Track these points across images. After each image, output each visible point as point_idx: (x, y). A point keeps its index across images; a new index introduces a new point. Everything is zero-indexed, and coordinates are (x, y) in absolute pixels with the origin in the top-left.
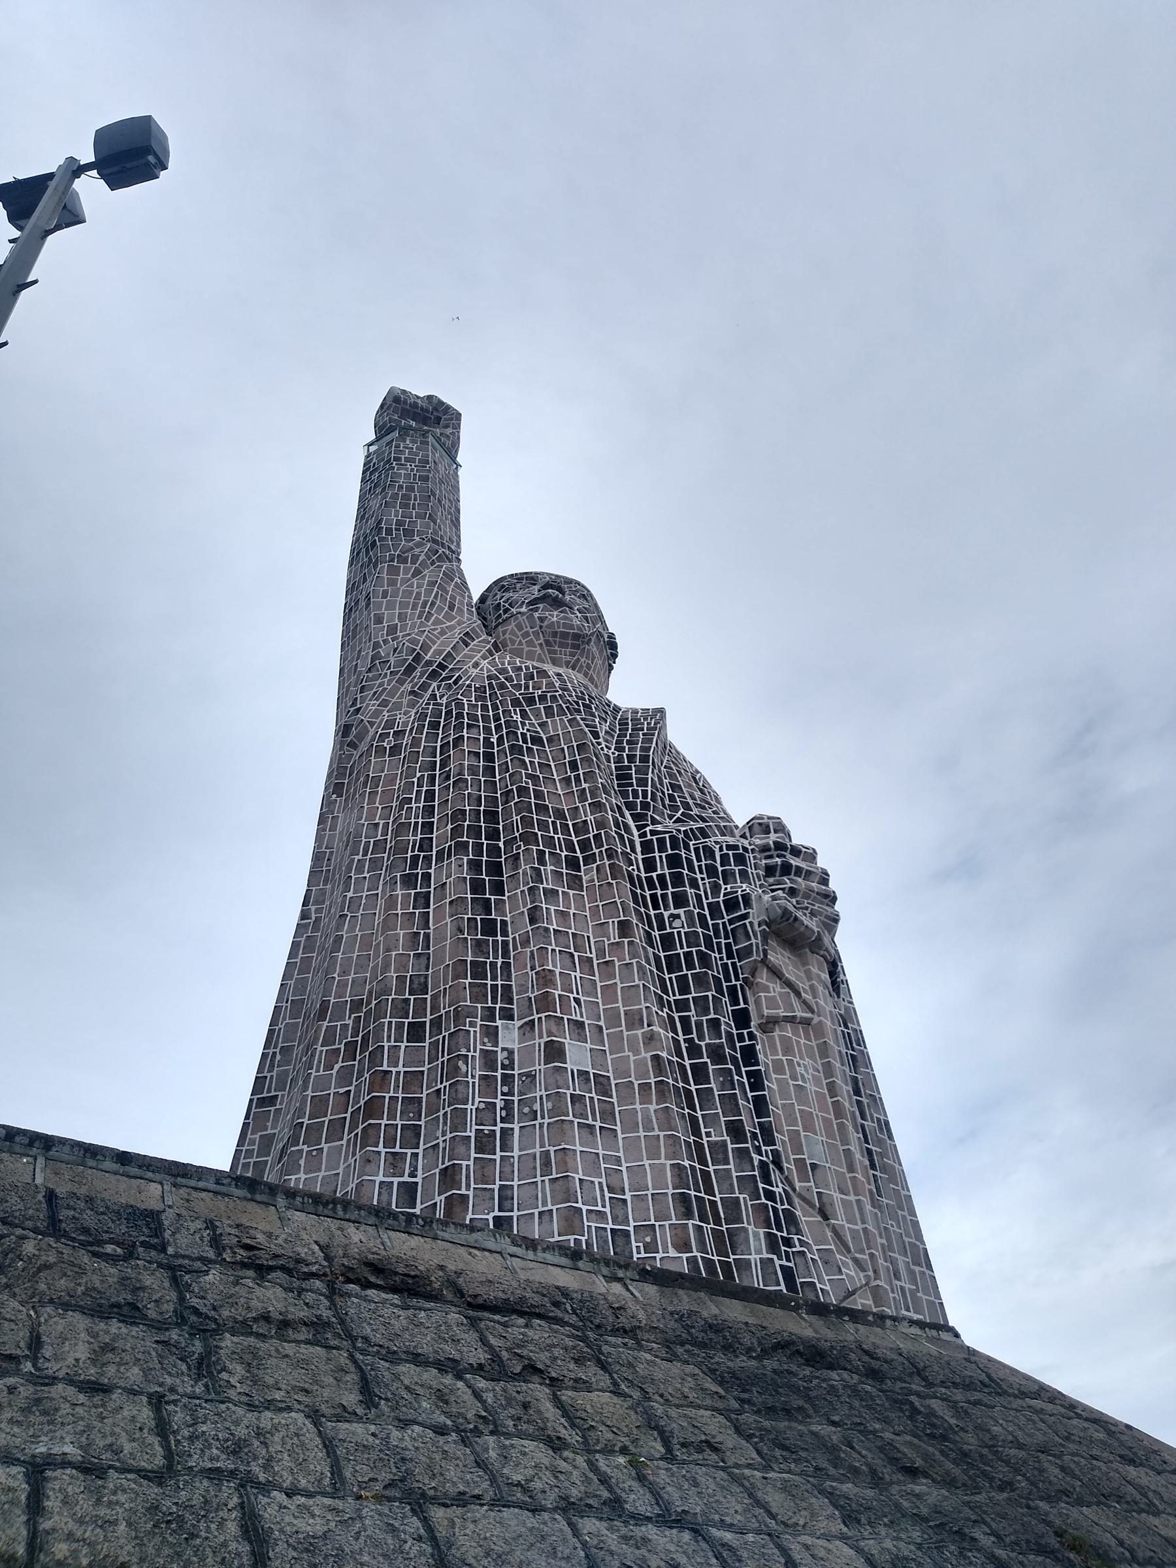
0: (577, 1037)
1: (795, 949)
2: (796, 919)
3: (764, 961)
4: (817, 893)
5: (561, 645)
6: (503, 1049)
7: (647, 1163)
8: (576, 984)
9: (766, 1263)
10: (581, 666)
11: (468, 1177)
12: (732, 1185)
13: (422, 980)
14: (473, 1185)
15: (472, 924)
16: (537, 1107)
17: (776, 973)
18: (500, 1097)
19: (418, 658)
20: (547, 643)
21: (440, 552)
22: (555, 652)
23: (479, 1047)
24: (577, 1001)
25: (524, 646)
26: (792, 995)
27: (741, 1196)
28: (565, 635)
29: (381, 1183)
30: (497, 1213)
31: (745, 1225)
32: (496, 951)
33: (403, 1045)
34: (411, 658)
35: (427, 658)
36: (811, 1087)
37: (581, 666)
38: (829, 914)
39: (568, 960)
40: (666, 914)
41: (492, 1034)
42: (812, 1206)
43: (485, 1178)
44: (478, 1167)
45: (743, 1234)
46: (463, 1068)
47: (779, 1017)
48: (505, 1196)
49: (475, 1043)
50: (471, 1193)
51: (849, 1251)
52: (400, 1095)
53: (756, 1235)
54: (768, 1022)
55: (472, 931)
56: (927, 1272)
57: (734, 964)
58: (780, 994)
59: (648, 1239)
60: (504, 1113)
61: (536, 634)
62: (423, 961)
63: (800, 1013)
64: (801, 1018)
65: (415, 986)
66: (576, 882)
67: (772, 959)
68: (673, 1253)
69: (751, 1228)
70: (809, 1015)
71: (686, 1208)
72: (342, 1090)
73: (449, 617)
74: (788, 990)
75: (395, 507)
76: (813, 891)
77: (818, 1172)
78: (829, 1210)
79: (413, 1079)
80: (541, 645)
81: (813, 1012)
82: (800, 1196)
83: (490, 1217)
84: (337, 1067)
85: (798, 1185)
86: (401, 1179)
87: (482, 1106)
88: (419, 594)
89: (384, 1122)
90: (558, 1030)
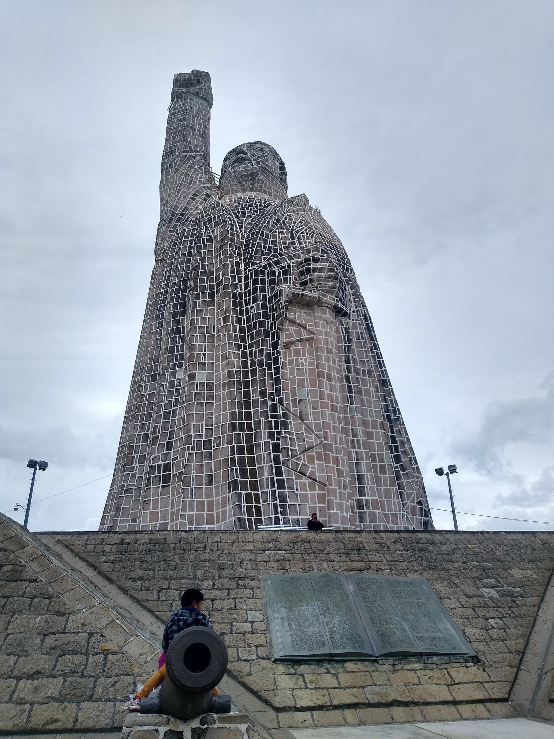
0: (202, 369)
1: (312, 306)
2: (302, 295)
3: (286, 318)
4: (324, 278)
5: (246, 181)
6: (177, 379)
7: (221, 413)
8: (205, 347)
9: (267, 443)
10: (256, 188)
11: (159, 429)
12: (258, 415)
13: (158, 357)
14: (161, 432)
15: (172, 332)
16: (184, 400)
17: (292, 322)
18: (174, 398)
19: (173, 214)
20: (240, 182)
21: (188, 155)
22: (244, 185)
23: (168, 380)
24: (204, 355)
25: (230, 188)
26: (302, 329)
27: (261, 419)
28: (246, 176)
29: (138, 435)
30: (168, 440)
31: (261, 430)
32: (179, 340)
33: (149, 384)
34: (170, 215)
35: (177, 212)
36: (307, 368)
37: (256, 188)
38: (330, 286)
39: (203, 338)
40: (249, 307)
41: (174, 374)
42: (297, 417)
43: (165, 429)
44: (163, 425)
45: (260, 433)
46: (162, 389)
47: (293, 341)
48: (172, 434)
49: (167, 378)
50: (160, 435)
51: (313, 432)
52: (147, 403)
53: (265, 433)
54: (287, 345)
55: (171, 334)
56: (403, 426)
57: (275, 323)
58: (295, 331)
59: (218, 442)
60: (175, 404)
61: (233, 180)
62: (159, 349)
63: (305, 336)
64: (306, 338)
65: (155, 360)
66: (212, 303)
67: (290, 316)
68: (226, 445)
69: (263, 431)
70: (312, 336)
71: (233, 428)
72: (135, 403)
73: (188, 188)
74: (300, 328)
75: (170, 140)
76: (322, 277)
77: (302, 403)
78: (304, 417)
79: (152, 395)
80: (236, 185)
81: (314, 334)
82: (292, 414)
83: (165, 442)
84: (135, 394)
85: (291, 410)
86: (144, 433)
87: (167, 402)
88: (176, 181)
89: (140, 413)
90: (194, 368)
